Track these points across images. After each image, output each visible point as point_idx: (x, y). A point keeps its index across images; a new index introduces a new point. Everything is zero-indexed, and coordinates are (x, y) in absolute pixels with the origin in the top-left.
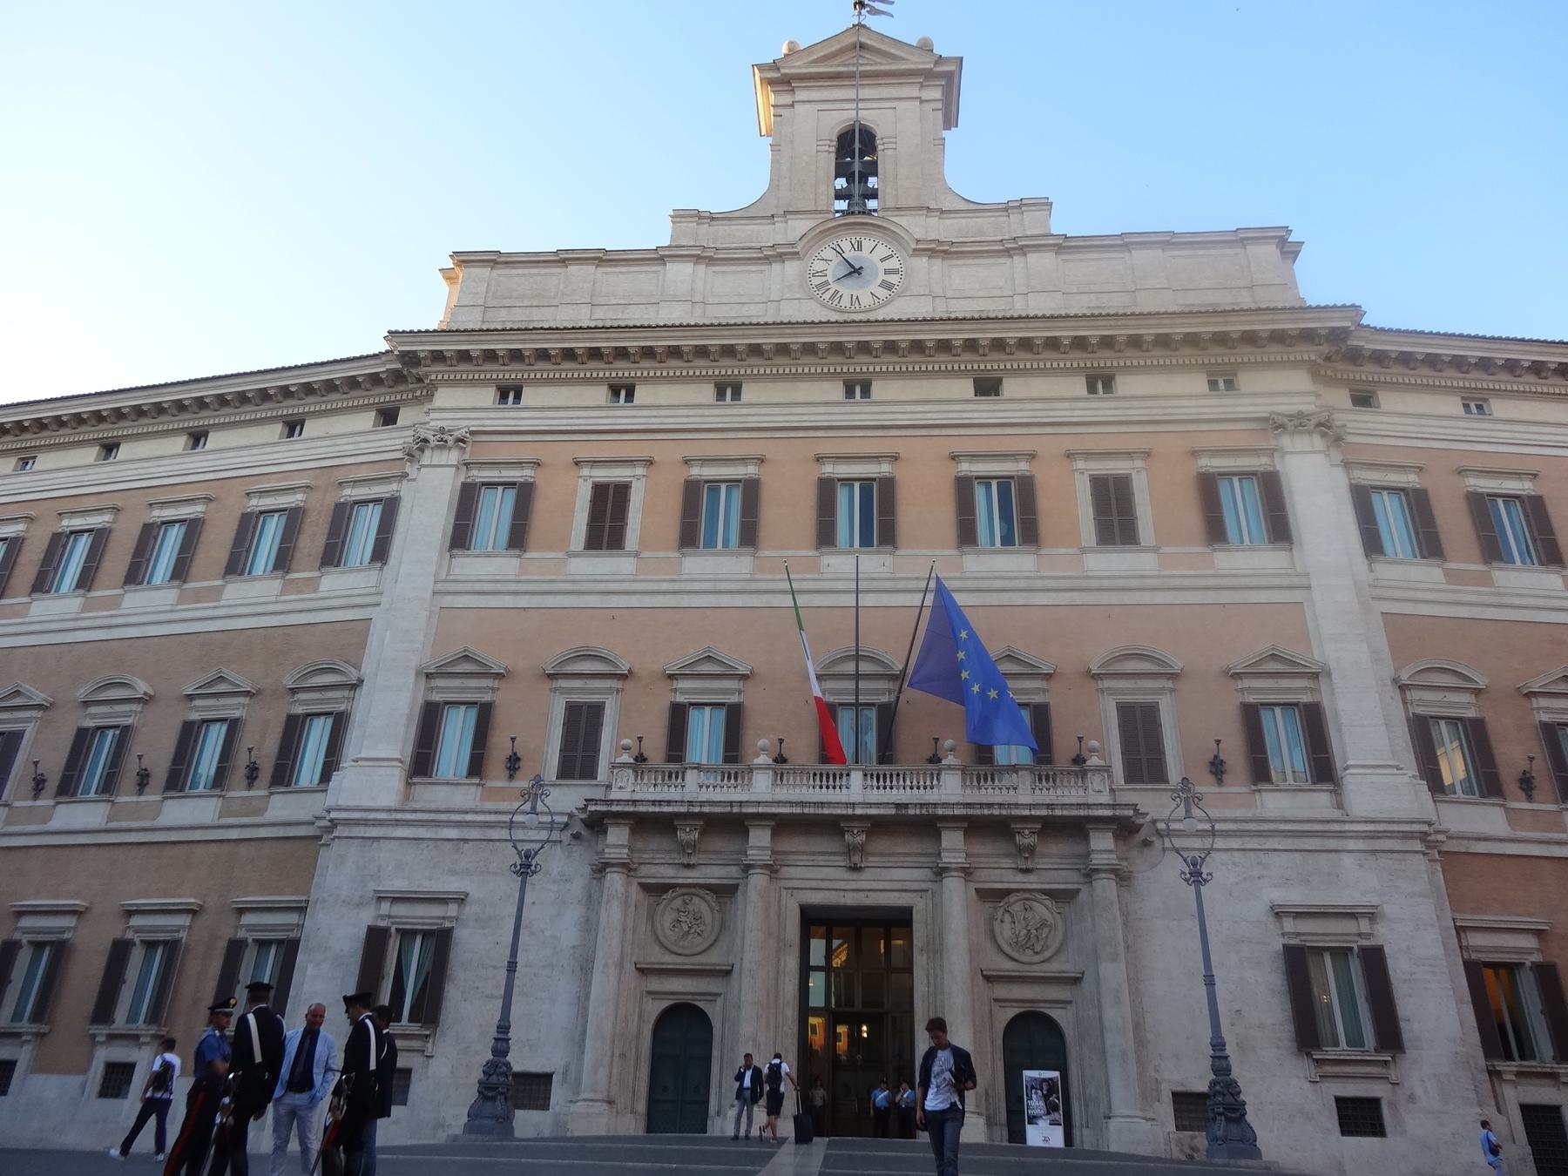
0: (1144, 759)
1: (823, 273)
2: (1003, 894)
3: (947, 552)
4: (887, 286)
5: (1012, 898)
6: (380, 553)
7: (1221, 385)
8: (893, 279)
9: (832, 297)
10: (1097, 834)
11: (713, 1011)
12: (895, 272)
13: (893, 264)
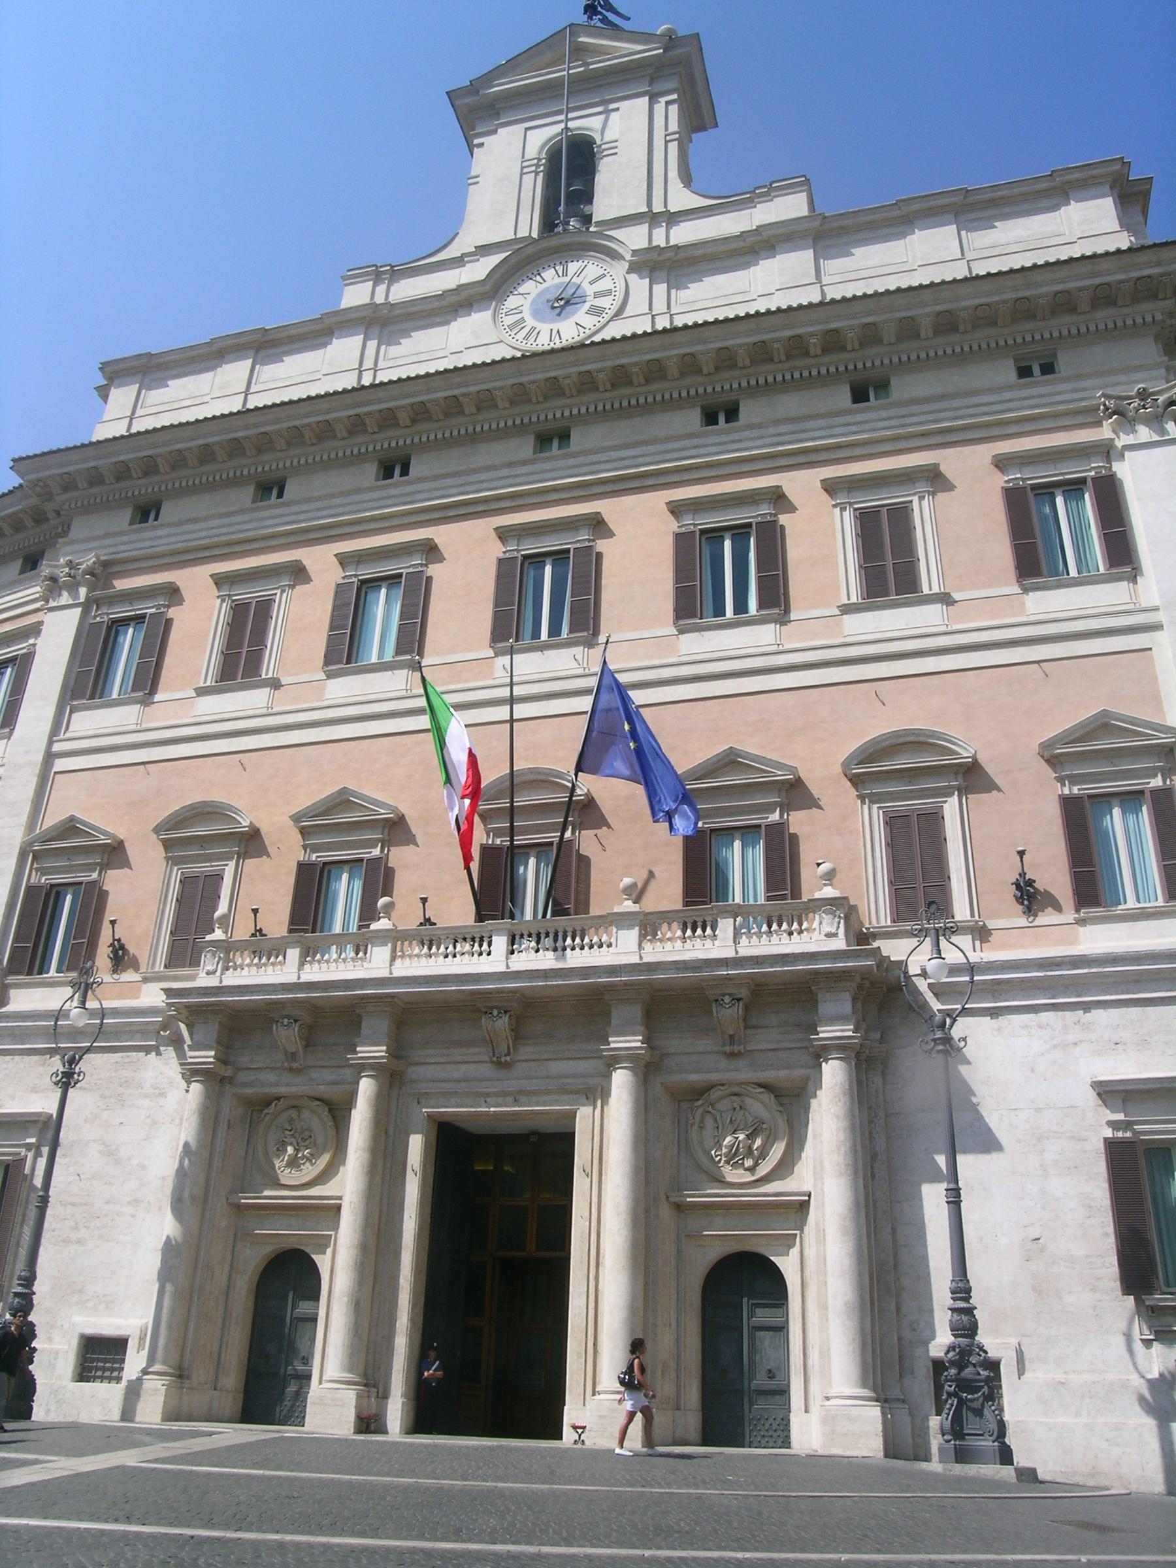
0: (920, 887)
1: (518, 310)
2: (701, 1091)
5: (715, 1094)
7: (1036, 370)
8: (604, 302)
9: (526, 338)
10: (828, 995)
12: (608, 293)
13: (605, 285)
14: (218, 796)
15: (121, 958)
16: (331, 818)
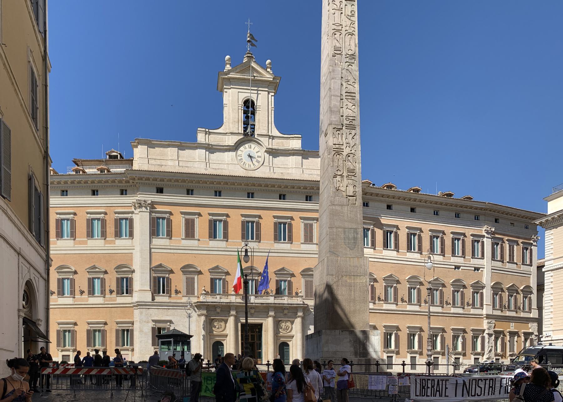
1: (240, 156)
3: (271, 242)
4: (258, 162)
6: (131, 235)
8: (259, 159)
11: (224, 343)
12: (260, 157)
13: (259, 154)
14: (191, 263)
15: (177, 292)
16: (215, 270)
